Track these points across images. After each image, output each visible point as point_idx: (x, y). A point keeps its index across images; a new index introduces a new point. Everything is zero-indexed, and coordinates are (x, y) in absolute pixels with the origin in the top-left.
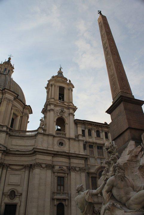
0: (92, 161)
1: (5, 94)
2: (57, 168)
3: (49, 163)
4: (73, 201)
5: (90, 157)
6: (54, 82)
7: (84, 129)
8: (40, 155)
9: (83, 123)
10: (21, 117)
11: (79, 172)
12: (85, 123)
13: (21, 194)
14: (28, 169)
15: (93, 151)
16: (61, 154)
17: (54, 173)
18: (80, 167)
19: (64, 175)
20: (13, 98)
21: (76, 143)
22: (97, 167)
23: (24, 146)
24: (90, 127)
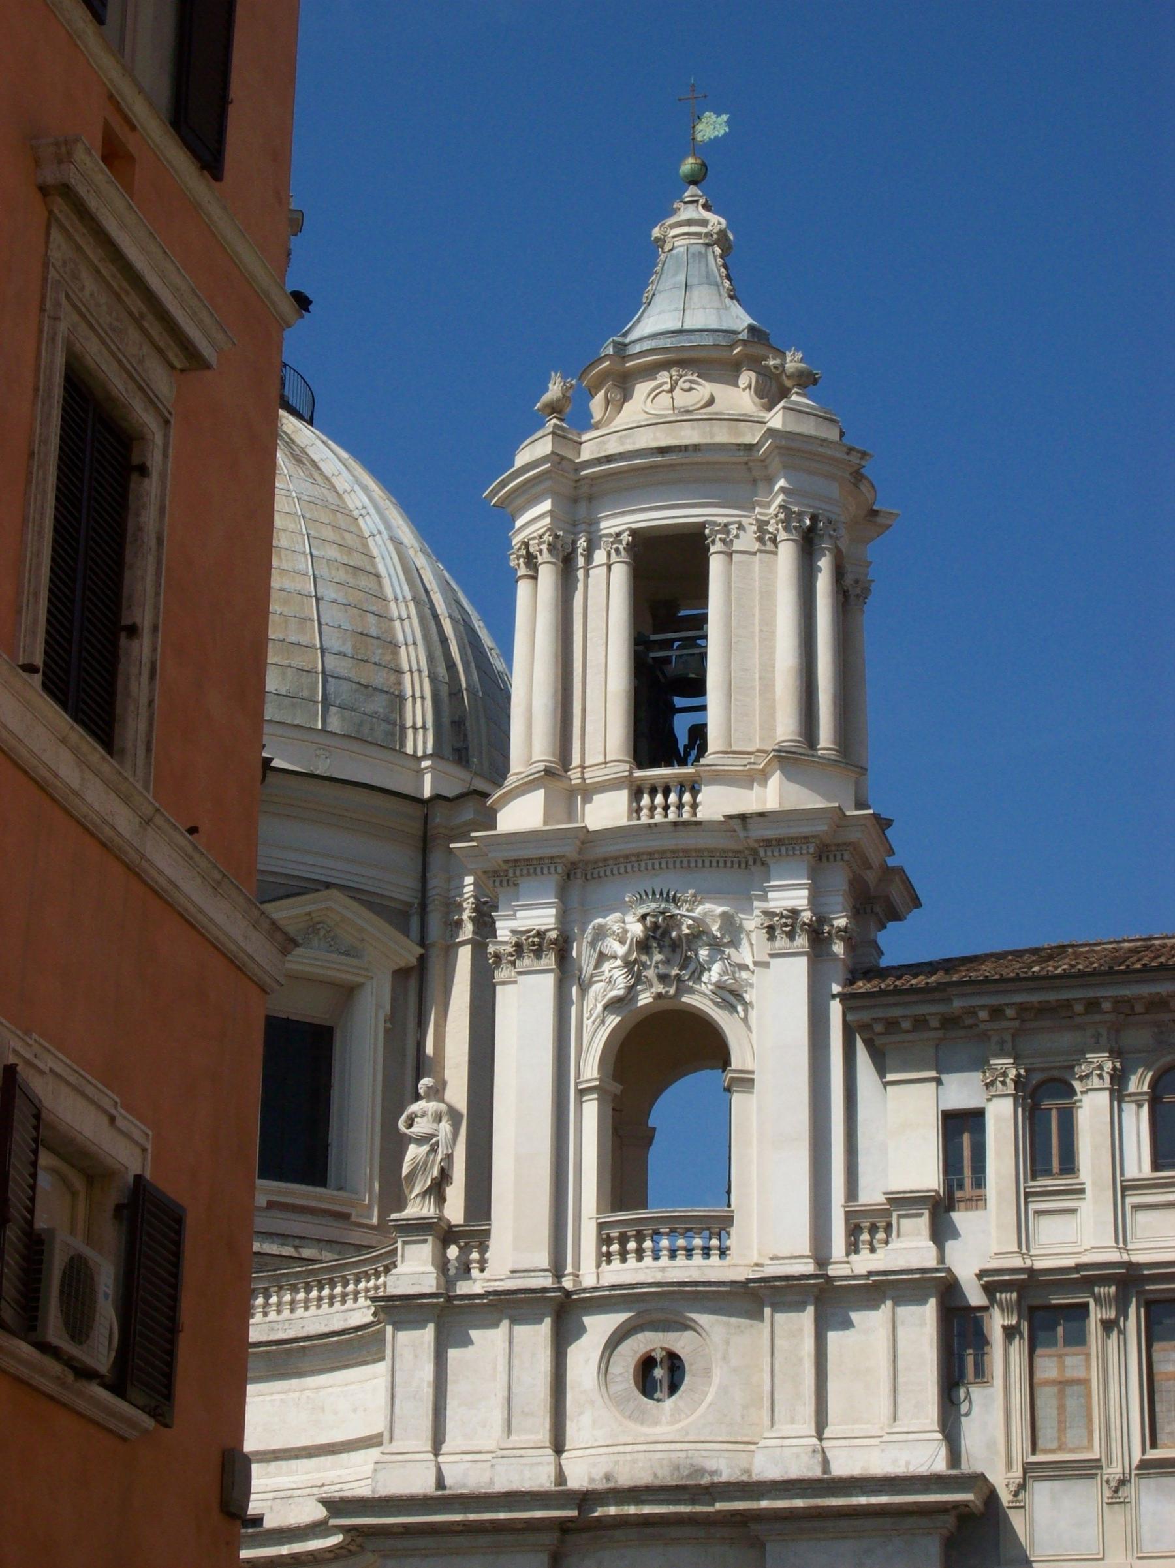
9: (949, 1022)
10: (401, 975)
12: (972, 1012)
15: (1086, 1382)
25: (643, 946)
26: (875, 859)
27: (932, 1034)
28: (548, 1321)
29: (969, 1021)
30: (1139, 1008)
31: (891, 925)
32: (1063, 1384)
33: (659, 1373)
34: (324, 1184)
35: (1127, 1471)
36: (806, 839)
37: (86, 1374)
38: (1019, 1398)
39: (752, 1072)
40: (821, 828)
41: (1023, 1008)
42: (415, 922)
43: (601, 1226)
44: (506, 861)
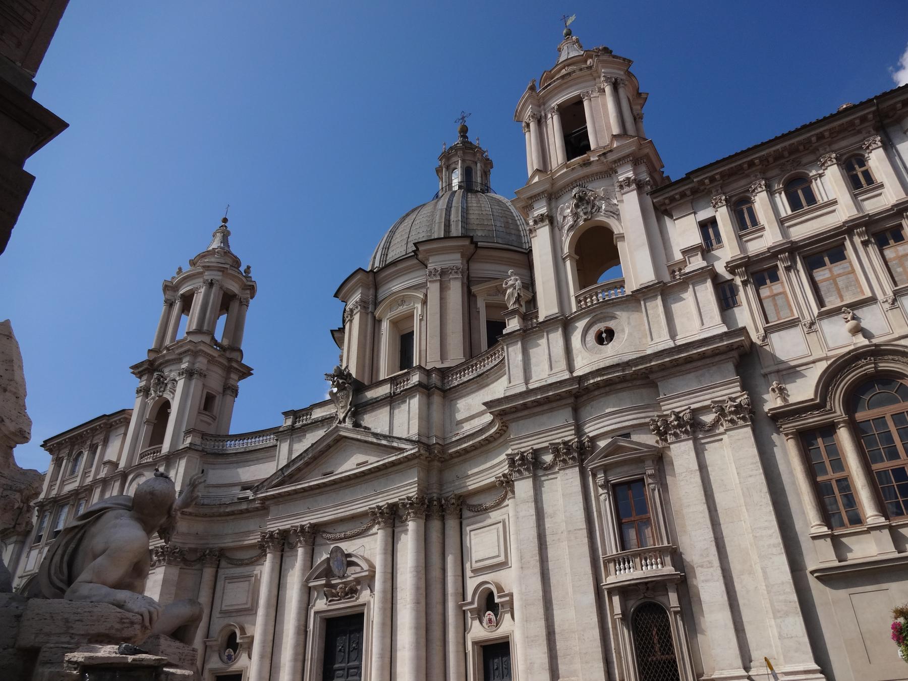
1: (428, 260)
4: (707, 581)
5: (768, 331)
7: (704, 214)
9: (694, 191)
12: (701, 182)
13: (511, 595)
15: (784, 293)
17: (594, 476)
20: (458, 256)
25: (577, 206)
26: (658, 169)
27: (688, 199)
28: (560, 329)
29: (702, 188)
30: (771, 159)
32: (773, 297)
33: (604, 335)
35: (813, 319)
36: (628, 156)
39: (623, 234)
41: (723, 175)
42: (530, 288)
43: (576, 297)
44: (528, 198)
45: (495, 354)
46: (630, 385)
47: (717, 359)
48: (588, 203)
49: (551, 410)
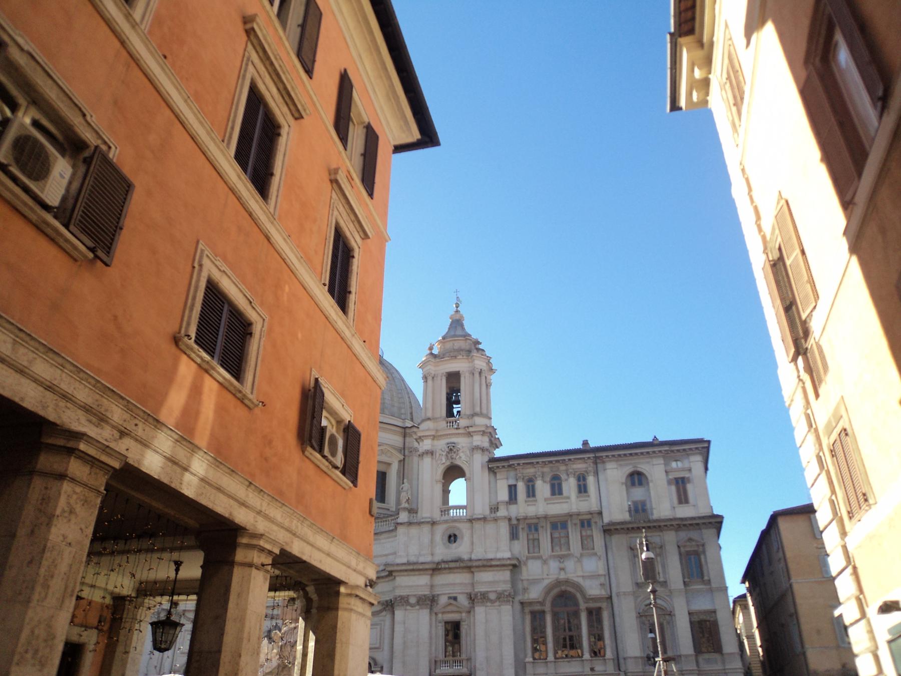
0: (532, 569)
2: (443, 600)
3: (422, 593)
5: (528, 558)
6: (428, 368)
7: (512, 482)
8: (403, 578)
9: (510, 466)
11: (497, 603)
12: (514, 464)
14: (389, 610)
15: (538, 539)
16: (447, 566)
17: (436, 614)
18: (496, 591)
19: (460, 614)
21: (490, 528)
22: (546, 582)
23: (381, 556)
24: (530, 471)
26: (493, 435)
31: (497, 449)
32: (534, 540)
33: (452, 538)
34: (384, 503)
36: (480, 431)
37: (336, 468)
38: (526, 542)
40: (483, 429)
42: (403, 451)
45: (386, 521)
46: (461, 571)
47: (503, 568)
48: (454, 453)
49: (420, 575)
